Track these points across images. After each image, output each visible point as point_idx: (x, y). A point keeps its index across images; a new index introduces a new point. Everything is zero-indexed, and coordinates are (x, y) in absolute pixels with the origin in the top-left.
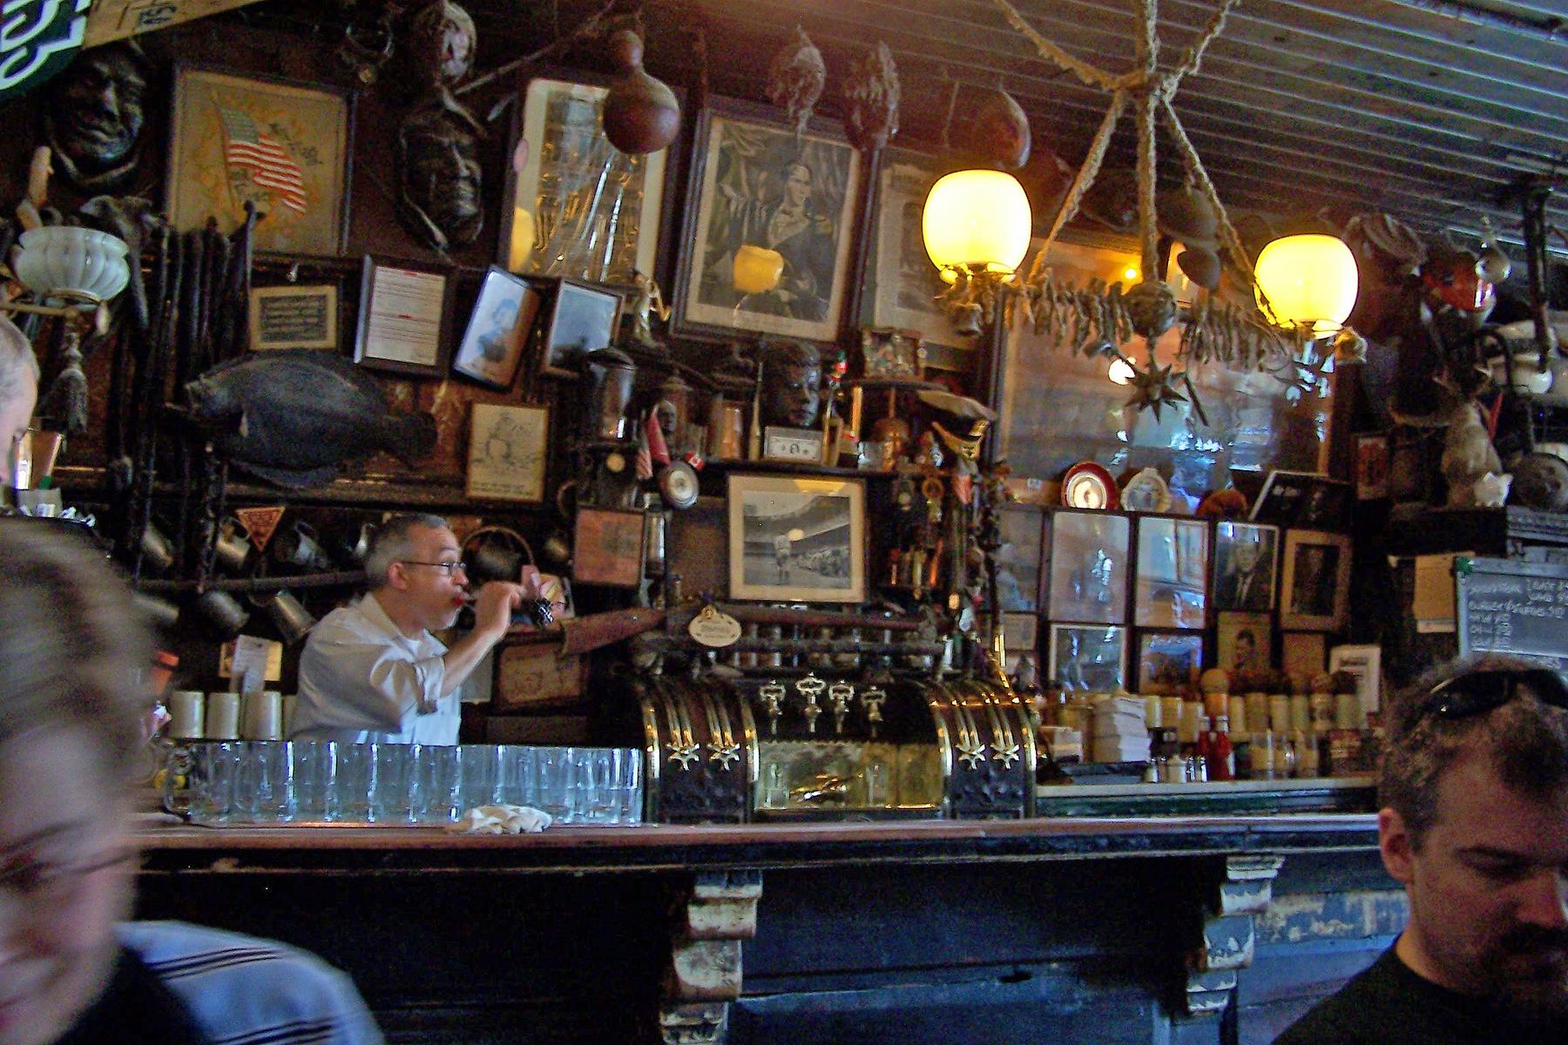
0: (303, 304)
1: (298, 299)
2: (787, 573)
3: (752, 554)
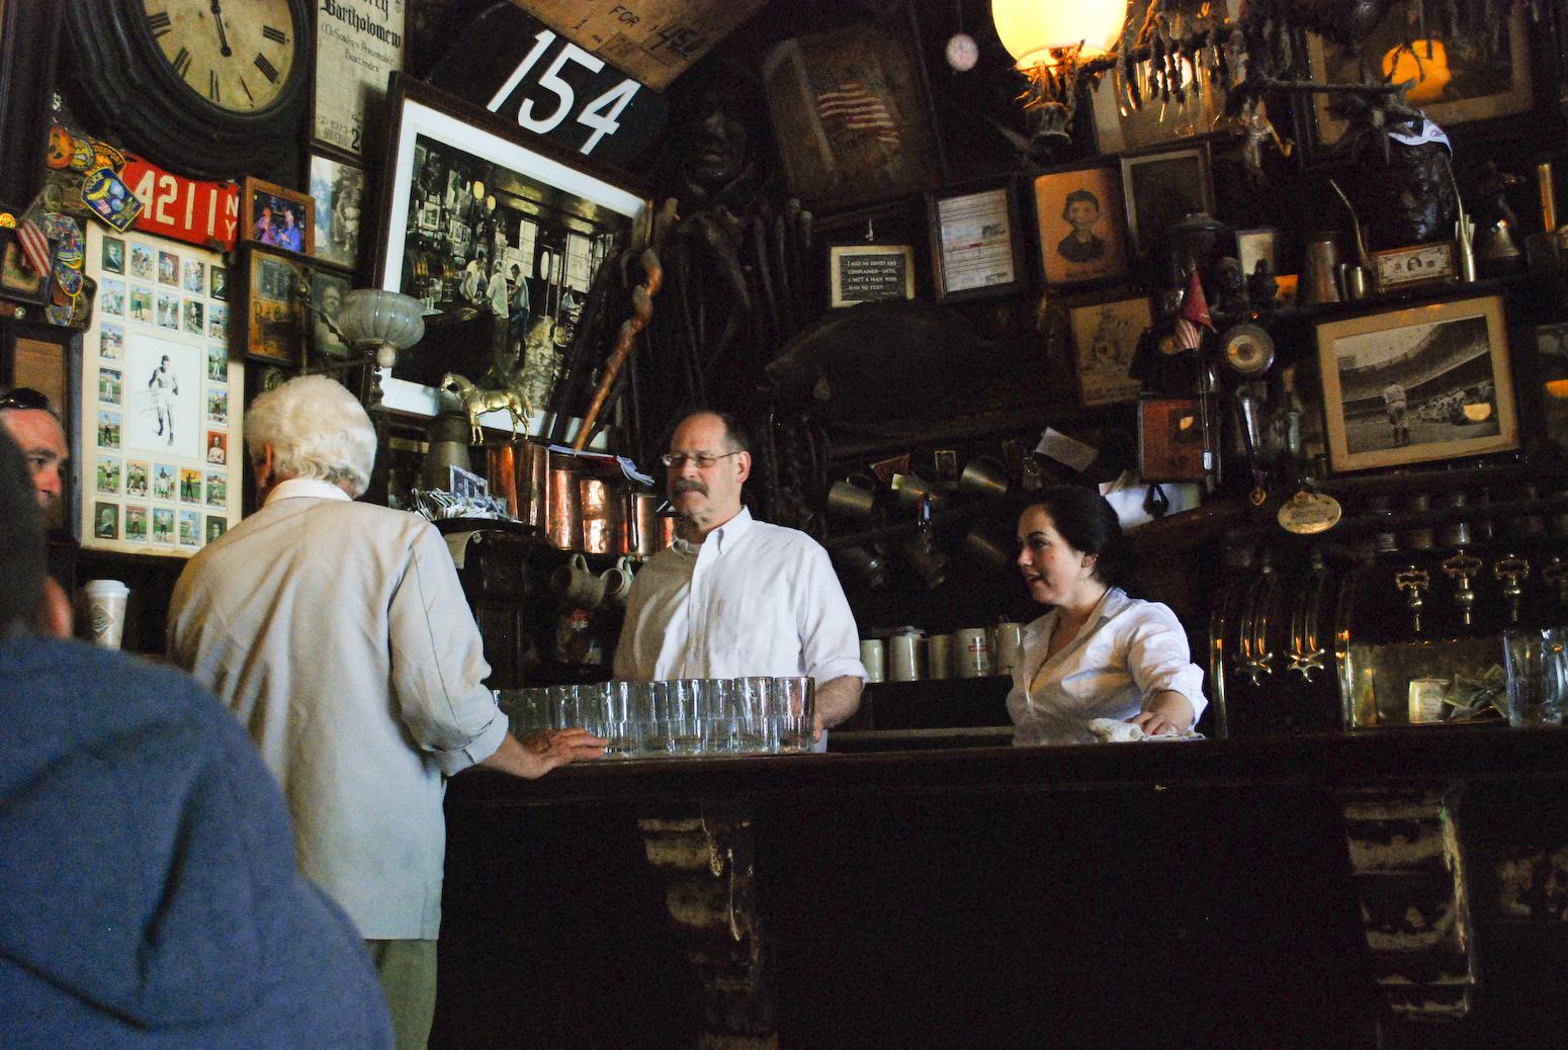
0: (881, 263)
1: (877, 258)
2: (1405, 431)
3: (1356, 416)
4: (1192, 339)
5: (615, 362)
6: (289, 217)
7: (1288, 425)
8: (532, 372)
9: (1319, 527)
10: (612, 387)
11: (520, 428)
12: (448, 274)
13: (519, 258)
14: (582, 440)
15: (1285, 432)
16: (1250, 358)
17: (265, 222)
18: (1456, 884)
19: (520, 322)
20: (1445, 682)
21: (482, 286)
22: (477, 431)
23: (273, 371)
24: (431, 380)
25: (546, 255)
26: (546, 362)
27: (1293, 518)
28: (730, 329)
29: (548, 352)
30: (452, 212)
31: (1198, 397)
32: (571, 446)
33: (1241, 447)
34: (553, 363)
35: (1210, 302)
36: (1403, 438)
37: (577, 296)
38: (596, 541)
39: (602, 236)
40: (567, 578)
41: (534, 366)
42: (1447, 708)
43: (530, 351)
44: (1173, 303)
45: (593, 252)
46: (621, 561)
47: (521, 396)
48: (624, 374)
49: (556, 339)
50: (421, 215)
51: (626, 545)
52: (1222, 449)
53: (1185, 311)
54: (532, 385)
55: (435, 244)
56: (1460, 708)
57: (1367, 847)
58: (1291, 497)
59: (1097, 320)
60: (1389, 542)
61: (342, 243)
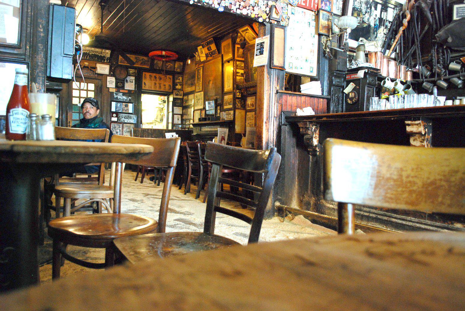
5: (398, 37)
6: (328, 3)
8: (379, 39)
10: (397, 42)
12: (361, 16)
13: (377, 13)
17: (323, 5)
19: (376, 28)
21: (368, 19)
23: (324, 36)
24: (357, 40)
25: (383, 12)
26: (382, 37)
28: (427, 27)
29: (383, 35)
30: (363, 2)
37: (390, 22)
39: (396, 8)
40: (384, 83)
45: (394, 12)
48: (400, 40)
50: (356, 3)
55: (359, 9)
61: (339, 9)
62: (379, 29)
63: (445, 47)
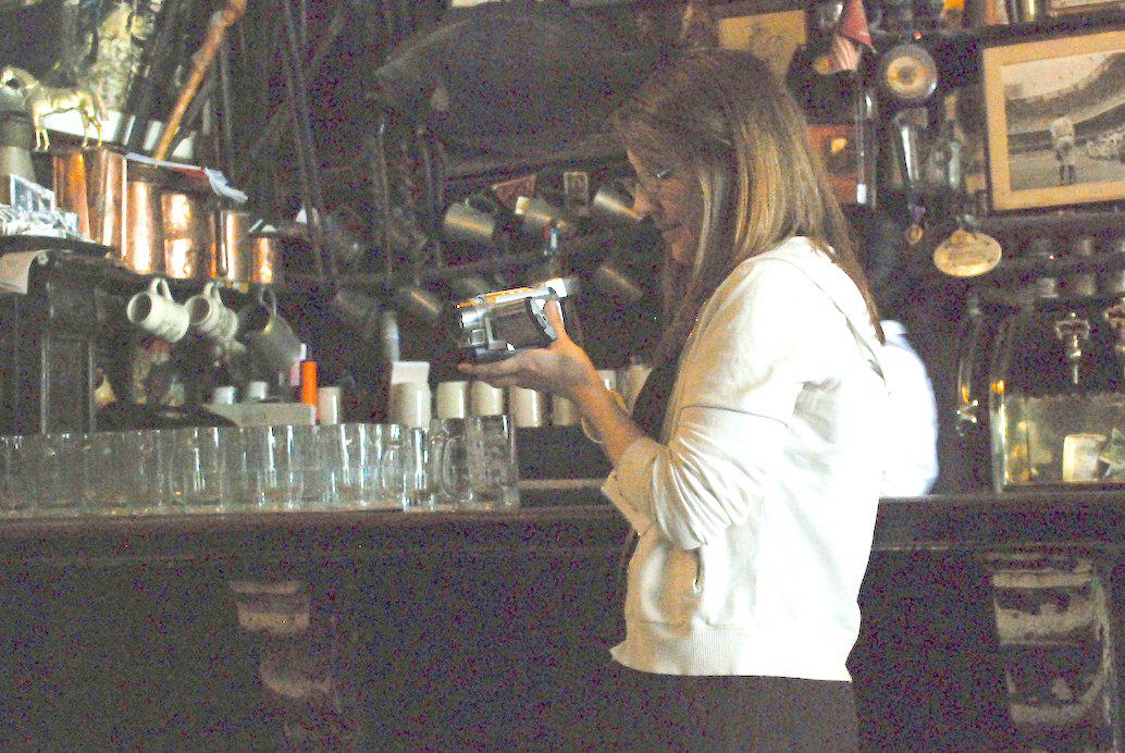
2: (1071, 168)
4: (849, 59)
5: (203, 59)
7: (948, 156)
8: (106, 68)
9: (977, 269)
10: (201, 85)
11: (92, 133)
14: (163, 148)
15: (944, 164)
16: (911, 82)
18: (1105, 656)
20: (1101, 438)
22: (42, 138)
26: (123, 56)
27: (950, 258)
29: (125, 44)
31: (851, 123)
32: (151, 154)
33: (898, 181)
34: (130, 58)
35: (870, 18)
36: (1068, 176)
38: (180, 265)
40: (145, 307)
41: (109, 61)
42: (1103, 467)
43: (104, 43)
44: (829, 18)
46: (208, 287)
47: (93, 95)
48: (214, 75)
49: (135, 30)
51: (214, 269)
52: (879, 182)
53: (840, 29)
54: (106, 83)
56: (1114, 466)
57: (1015, 616)
58: (949, 234)
59: (748, 32)
60: (1049, 288)
62: (104, 17)
63: (420, 132)
